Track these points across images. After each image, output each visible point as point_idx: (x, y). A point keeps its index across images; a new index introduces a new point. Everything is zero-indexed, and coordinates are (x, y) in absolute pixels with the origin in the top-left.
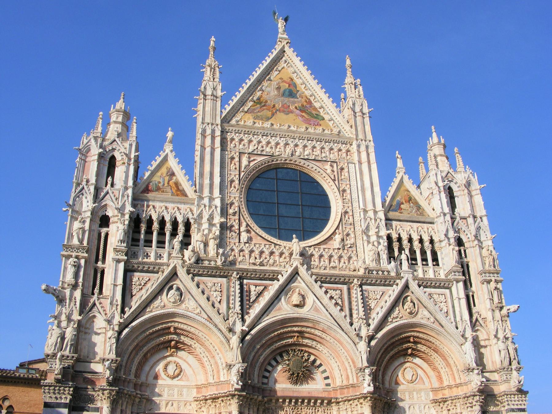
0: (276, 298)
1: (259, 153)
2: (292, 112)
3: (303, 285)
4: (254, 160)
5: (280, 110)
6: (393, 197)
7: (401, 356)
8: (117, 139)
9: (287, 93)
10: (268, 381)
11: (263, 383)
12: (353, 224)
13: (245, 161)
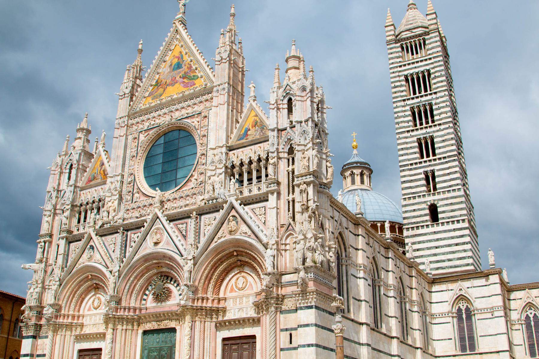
0: (144, 241)
1: (152, 127)
2: (177, 82)
3: (161, 226)
4: (148, 134)
5: (169, 85)
6: (242, 127)
7: (235, 267)
8: (73, 153)
9: (176, 67)
10: (146, 303)
11: (143, 305)
12: (205, 164)
13: (142, 137)
